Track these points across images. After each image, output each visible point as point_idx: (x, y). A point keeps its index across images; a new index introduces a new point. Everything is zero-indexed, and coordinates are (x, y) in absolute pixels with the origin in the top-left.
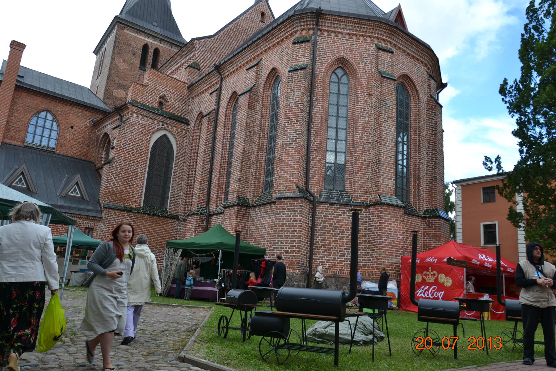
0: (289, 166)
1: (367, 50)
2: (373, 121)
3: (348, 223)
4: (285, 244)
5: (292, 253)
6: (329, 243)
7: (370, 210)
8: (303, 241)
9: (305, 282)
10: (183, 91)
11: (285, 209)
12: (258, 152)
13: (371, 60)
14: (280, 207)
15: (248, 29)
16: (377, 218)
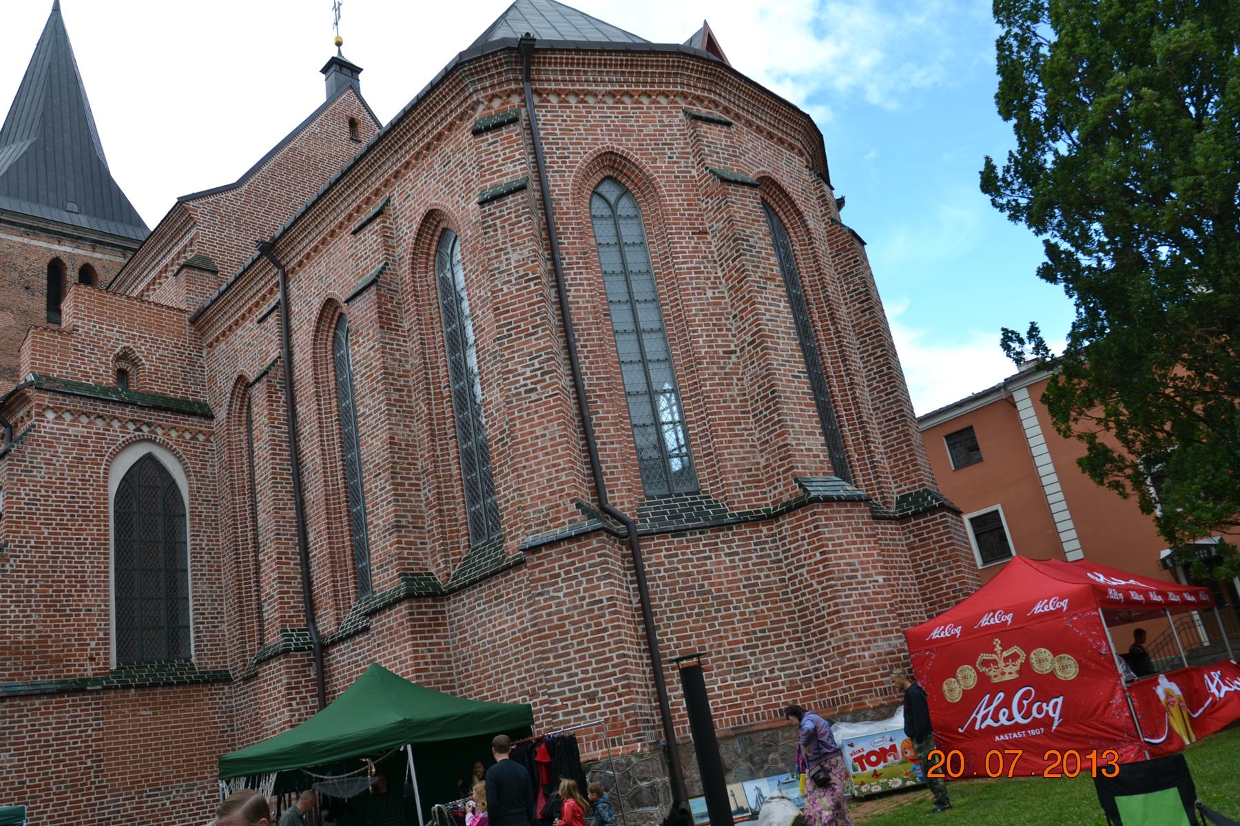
0: (540, 453)
2: (726, 295)
3: (734, 575)
4: (581, 676)
5: (611, 697)
6: (699, 642)
7: (783, 525)
8: (631, 653)
9: (664, 775)
10: (180, 334)
11: (558, 575)
12: (433, 441)
13: (683, 148)
14: (540, 572)
15: (322, 161)
16: (809, 544)
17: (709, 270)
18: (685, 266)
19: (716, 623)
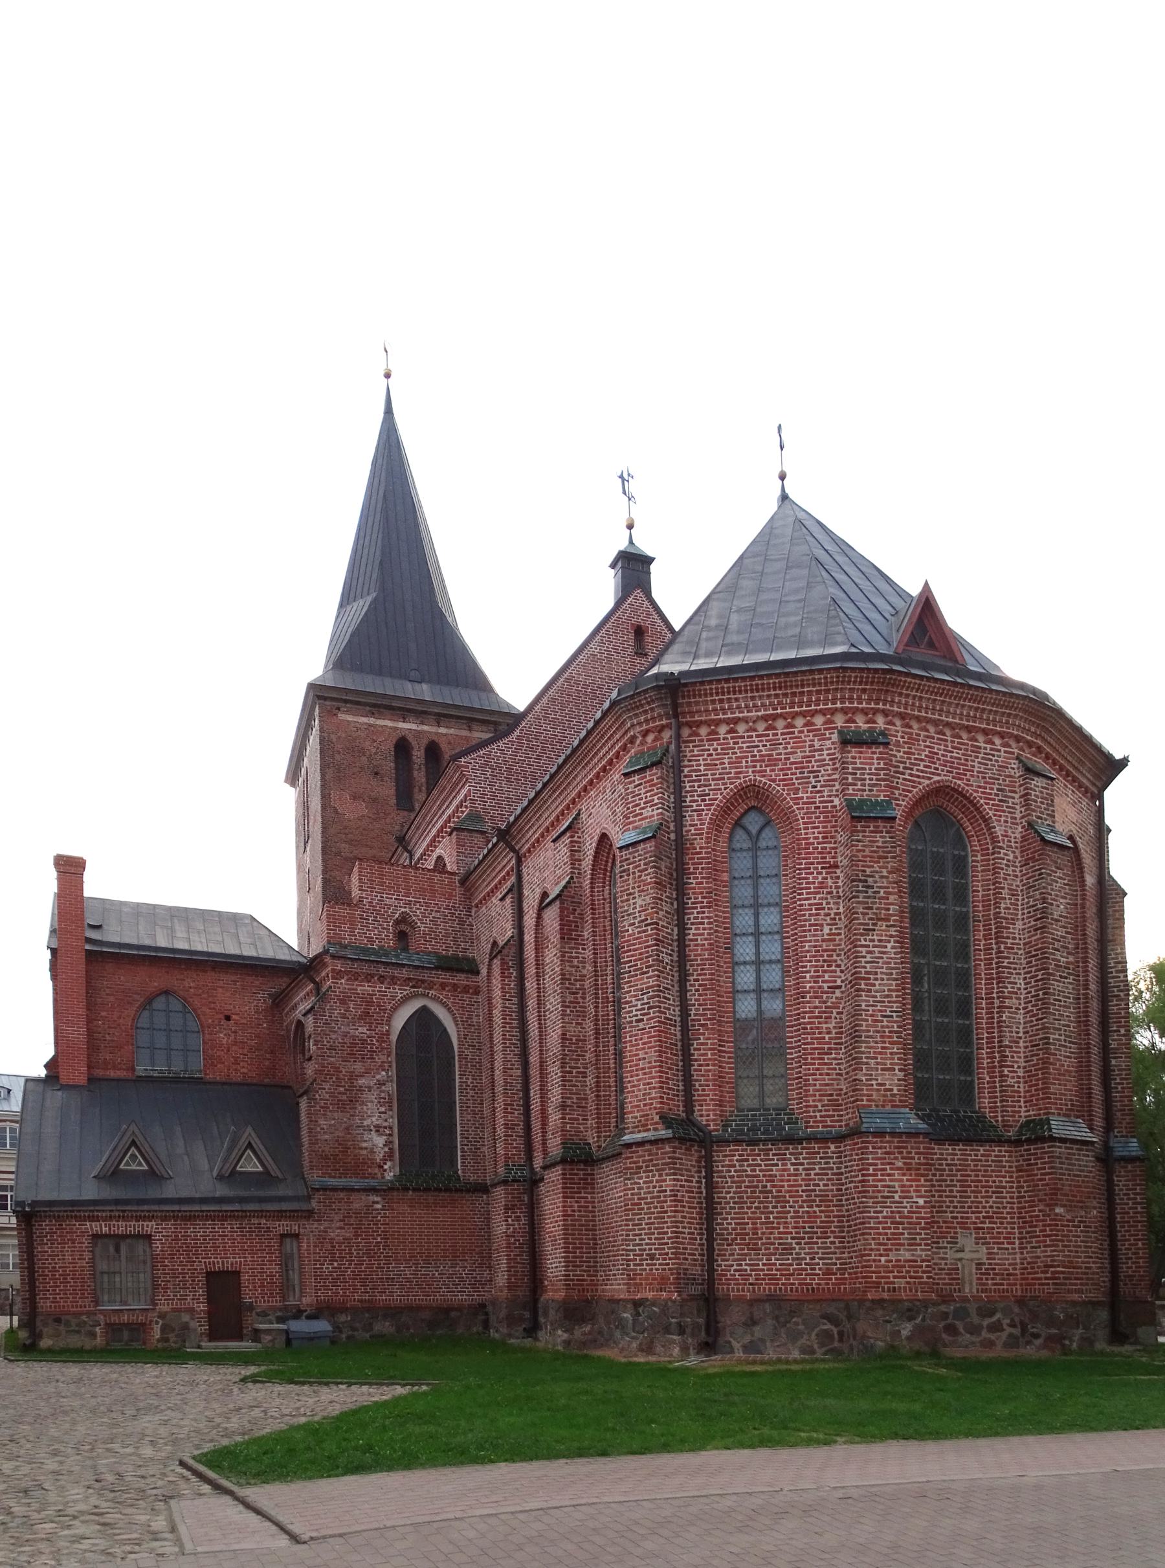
1: (815, 751)
2: (843, 931)
3: (795, 1181)
5: (664, 1259)
6: (753, 1229)
8: (687, 1231)
17: (832, 906)
18: (807, 902)
19: (771, 1216)
